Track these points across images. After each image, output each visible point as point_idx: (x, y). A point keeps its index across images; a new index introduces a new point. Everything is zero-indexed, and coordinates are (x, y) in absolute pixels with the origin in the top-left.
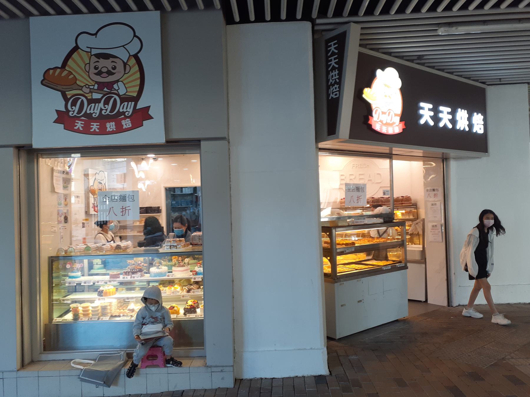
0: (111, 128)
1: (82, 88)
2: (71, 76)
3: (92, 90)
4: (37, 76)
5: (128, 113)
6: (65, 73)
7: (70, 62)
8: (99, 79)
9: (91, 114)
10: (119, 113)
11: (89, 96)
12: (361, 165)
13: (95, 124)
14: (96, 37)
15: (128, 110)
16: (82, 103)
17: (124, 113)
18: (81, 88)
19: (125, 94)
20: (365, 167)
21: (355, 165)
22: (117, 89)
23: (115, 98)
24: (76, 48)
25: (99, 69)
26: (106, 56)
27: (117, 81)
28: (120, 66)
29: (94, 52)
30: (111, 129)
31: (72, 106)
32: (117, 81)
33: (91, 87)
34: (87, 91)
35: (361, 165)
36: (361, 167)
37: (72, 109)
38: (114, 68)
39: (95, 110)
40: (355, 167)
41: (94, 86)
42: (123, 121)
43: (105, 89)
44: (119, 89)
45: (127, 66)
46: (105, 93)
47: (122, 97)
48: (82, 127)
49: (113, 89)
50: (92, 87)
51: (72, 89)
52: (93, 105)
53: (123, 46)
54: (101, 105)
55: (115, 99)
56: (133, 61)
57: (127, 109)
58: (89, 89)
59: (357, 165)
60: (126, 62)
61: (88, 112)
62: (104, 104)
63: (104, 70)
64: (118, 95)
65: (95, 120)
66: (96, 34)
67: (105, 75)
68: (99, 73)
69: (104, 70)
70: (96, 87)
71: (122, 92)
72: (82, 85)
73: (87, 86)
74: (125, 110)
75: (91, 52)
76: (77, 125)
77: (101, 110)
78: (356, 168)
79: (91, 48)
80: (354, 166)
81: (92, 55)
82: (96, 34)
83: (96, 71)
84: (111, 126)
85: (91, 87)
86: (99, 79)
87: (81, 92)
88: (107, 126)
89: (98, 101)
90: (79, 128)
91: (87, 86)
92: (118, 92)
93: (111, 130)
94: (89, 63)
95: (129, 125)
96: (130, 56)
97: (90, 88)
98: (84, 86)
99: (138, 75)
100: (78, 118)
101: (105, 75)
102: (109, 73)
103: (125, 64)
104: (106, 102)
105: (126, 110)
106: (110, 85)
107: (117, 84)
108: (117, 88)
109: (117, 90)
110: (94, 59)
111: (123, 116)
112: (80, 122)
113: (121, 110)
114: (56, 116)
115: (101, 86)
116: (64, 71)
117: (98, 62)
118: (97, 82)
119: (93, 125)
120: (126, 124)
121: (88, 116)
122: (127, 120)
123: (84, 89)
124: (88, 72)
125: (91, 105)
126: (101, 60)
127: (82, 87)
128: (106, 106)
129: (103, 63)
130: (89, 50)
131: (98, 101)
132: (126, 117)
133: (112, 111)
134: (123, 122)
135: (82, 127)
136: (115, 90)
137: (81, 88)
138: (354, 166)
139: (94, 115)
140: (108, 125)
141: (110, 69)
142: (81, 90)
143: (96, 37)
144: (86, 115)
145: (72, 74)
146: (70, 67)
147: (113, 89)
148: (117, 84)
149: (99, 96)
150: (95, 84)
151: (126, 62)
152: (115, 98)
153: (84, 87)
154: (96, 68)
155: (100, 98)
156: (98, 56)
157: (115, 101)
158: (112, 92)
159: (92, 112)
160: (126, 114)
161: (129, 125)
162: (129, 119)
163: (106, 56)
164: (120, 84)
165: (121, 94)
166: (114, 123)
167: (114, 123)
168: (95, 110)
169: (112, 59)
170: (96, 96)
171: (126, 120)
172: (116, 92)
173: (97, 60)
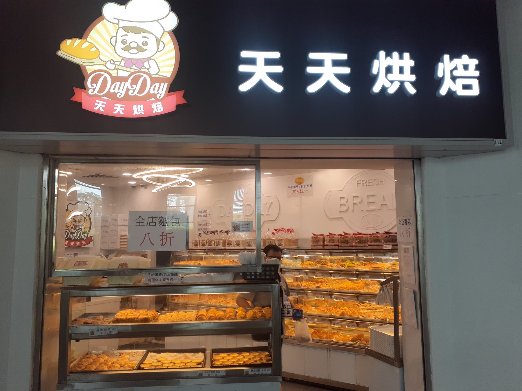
0: (138, 111)
1: (106, 64)
2: (94, 49)
3: (117, 67)
5: (159, 95)
8: (126, 54)
9: (115, 94)
10: (149, 96)
11: (114, 73)
12: (370, 181)
13: (119, 106)
14: (125, 8)
15: (159, 92)
16: (105, 80)
17: (154, 95)
18: (104, 63)
19: (157, 74)
20: (376, 184)
21: (361, 182)
22: (147, 68)
23: (145, 77)
25: (128, 44)
26: (137, 30)
28: (152, 42)
29: (122, 24)
30: (138, 112)
31: (92, 83)
32: (149, 59)
33: (116, 63)
34: (112, 67)
35: (370, 181)
36: (371, 184)
37: (93, 86)
38: (146, 44)
40: (362, 184)
41: (120, 62)
42: (154, 104)
43: (134, 67)
44: (150, 68)
45: (161, 43)
46: (133, 71)
47: (153, 76)
48: (103, 107)
49: (143, 67)
50: (118, 63)
51: (94, 64)
52: (118, 83)
53: (157, 21)
54: (128, 84)
55: (145, 80)
57: (158, 91)
58: (114, 65)
59: (364, 182)
60: (159, 38)
61: (112, 91)
62: (131, 84)
63: (135, 45)
64: (149, 75)
65: (120, 101)
67: (134, 51)
68: (128, 49)
69: (134, 45)
70: (123, 63)
71: (153, 71)
72: (106, 60)
73: (112, 62)
74: (156, 92)
75: (118, 24)
76: (97, 106)
77: (128, 90)
78: (363, 186)
79: (119, 20)
80: (360, 183)
81: (119, 28)
83: (124, 46)
84: (139, 109)
85: (116, 63)
86: (126, 54)
87: (104, 68)
88: (134, 109)
89: (125, 79)
90: (99, 108)
91: (112, 62)
92: (149, 71)
93: (139, 113)
94: (116, 36)
95: (160, 109)
96: (164, 32)
97: (115, 65)
98: (109, 61)
100: (100, 98)
101: (134, 51)
102: (140, 49)
103: (158, 41)
104: (135, 82)
105: (157, 92)
106: (140, 62)
107: (148, 62)
108: (148, 67)
109: (148, 69)
110: (121, 32)
111: (153, 99)
112: (101, 102)
113: (152, 92)
115: (129, 63)
116: (85, 42)
117: (127, 35)
118: (123, 58)
119: (117, 107)
120: (157, 108)
122: (159, 103)
123: (108, 65)
124: (115, 47)
125: (114, 84)
126: (130, 34)
127: (106, 62)
128: (133, 86)
129: (132, 37)
130: (116, 21)
131: (125, 79)
132: (157, 100)
133: (140, 92)
134: (154, 106)
135: (103, 107)
136: (146, 68)
137: (104, 63)
138: (360, 183)
139: (118, 95)
140: (135, 108)
141: (140, 44)
142: (105, 65)
143: (125, 8)
144: (108, 94)
145: (95, 46)
146: (92, 38)
147: (143, 67)
148: (148, 62)
149: (126, 74)
150: (121, 60)
151: (159, 38)
152: (145, 77)
153: (109, 62)
154: (124, 42)
155: (127, 76)
156: (127, 29)
157: (145, 81)
158: (142, 70)
159: (116, 91)
160: (158, 96)
161: (160, 109)
162: (161, 103)
163: (137, 30)
164: (151, 62)
165: (152, 73)
166: (142, 106)
167: (142, 106)
169: (143, 34)
170: (122, 74)
171: (157, 104)
172: (146, 71)
173: (126, 33)
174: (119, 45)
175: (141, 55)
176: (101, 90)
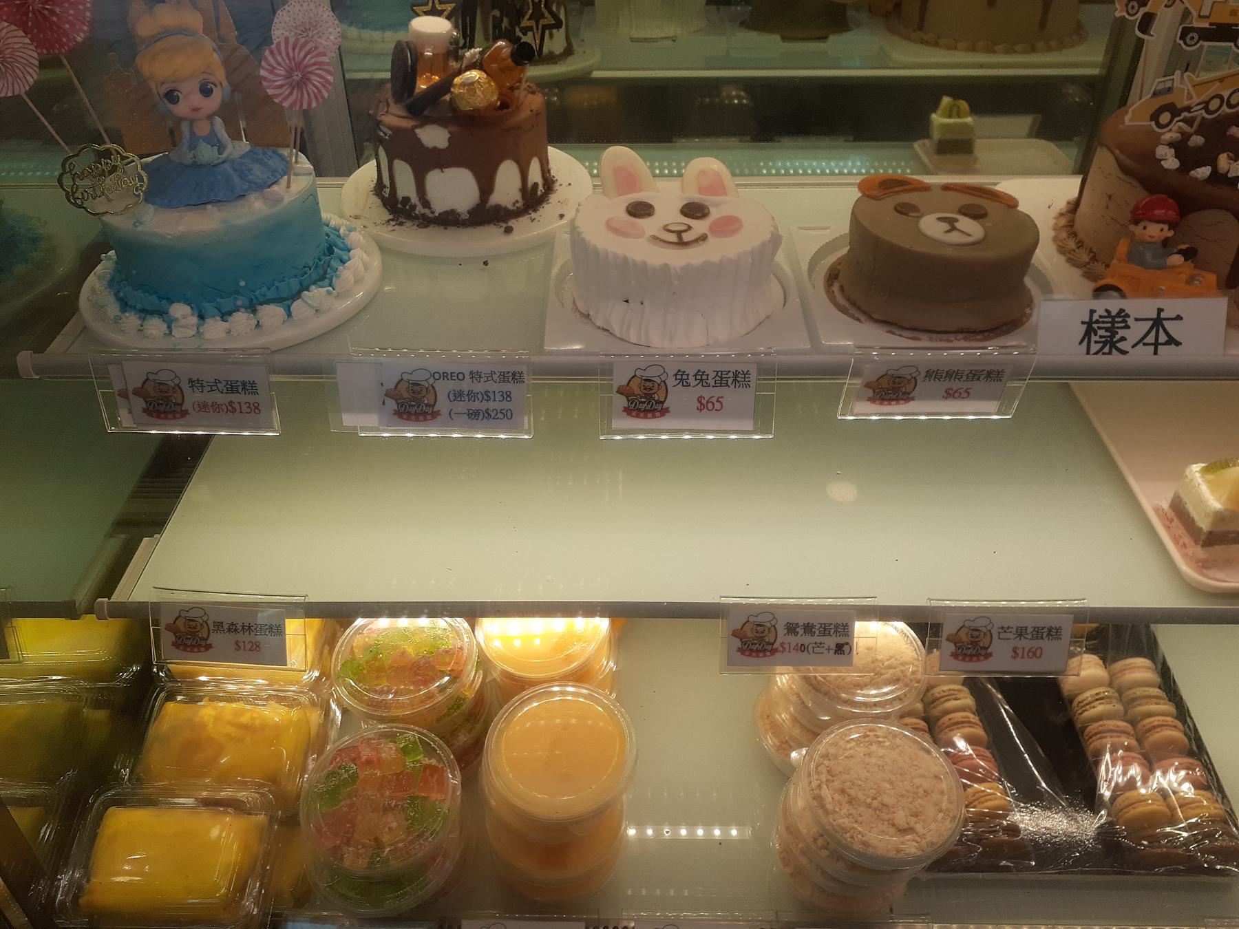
4: (615, 389)
6: (628, 388)
7: (631, 382)
8: (644, 391)
17: (656, 409)
24: (635, 375)
27: (654, 393)
28: (656, 386)
29: (643, 378)
34: (638, 396)
38: (653, 387)
39: (643, 407)
54: (646, 405)
56: (663, 384)
66: (645, 370)
71: (656, 399)
82: (645, 370)
89: (644, 402)
99: (665, 391)
103: (659, 385)
114: (623, 409)
121: (639, 410)
129: (648, 384)
131: (644, 402)
133: (651, 407)
154: (644, 386)
156: (645, 380)
157: (653, 403)
168: (643, 407)
174: (642, 387)
175: (651, 392)
176: (634, 407)
